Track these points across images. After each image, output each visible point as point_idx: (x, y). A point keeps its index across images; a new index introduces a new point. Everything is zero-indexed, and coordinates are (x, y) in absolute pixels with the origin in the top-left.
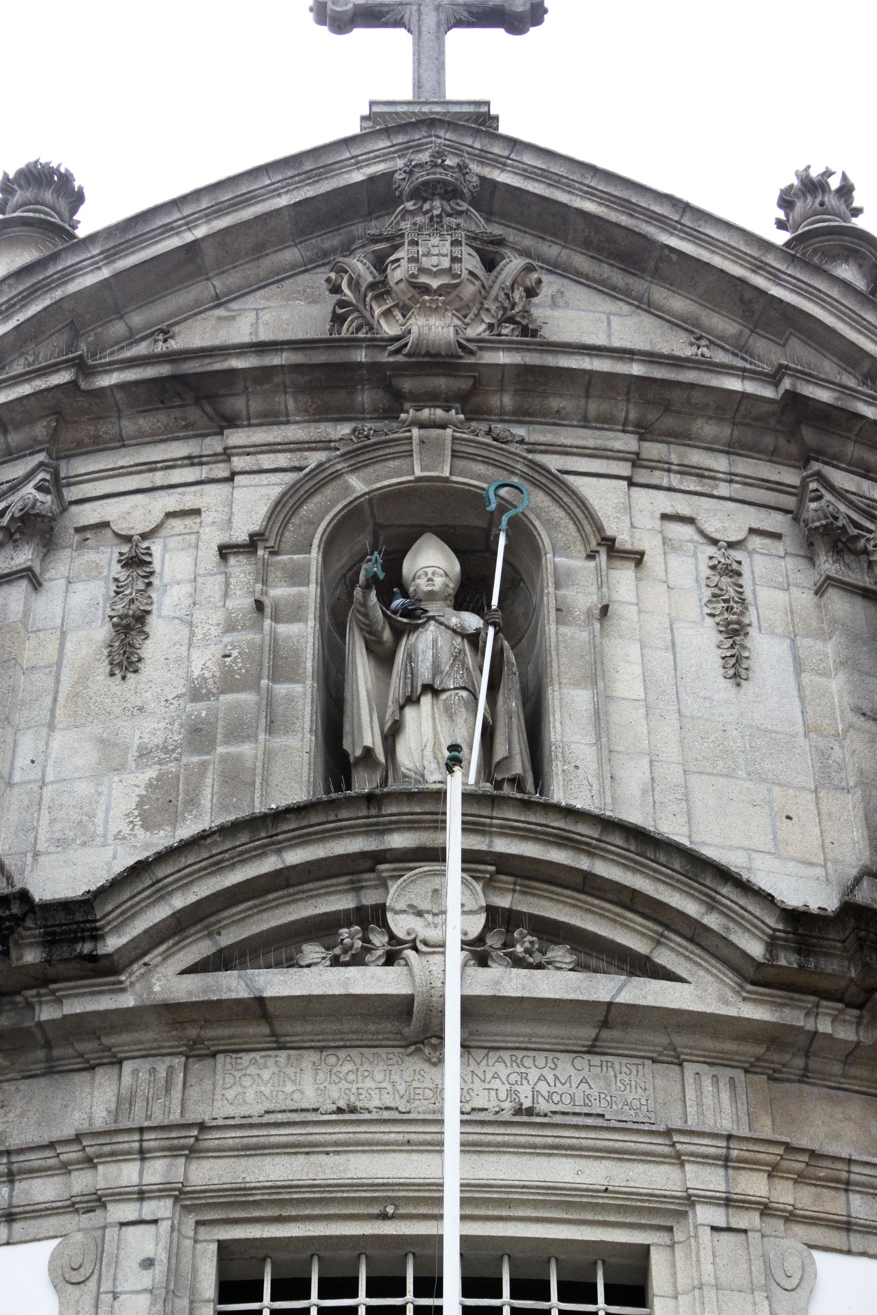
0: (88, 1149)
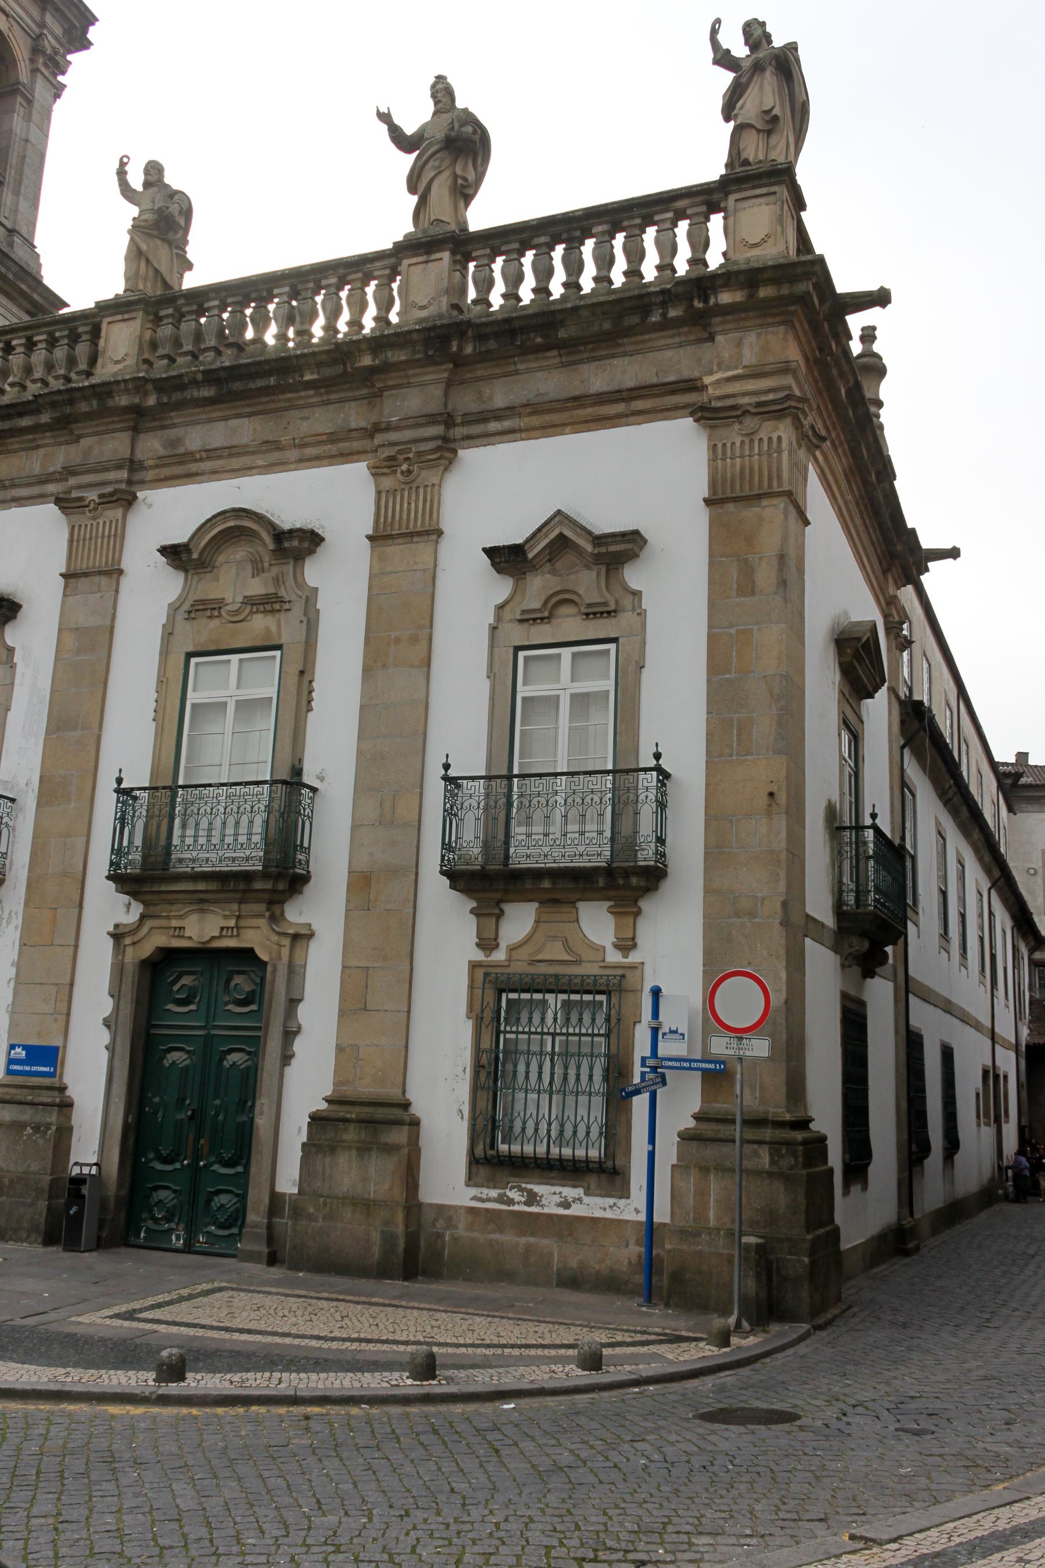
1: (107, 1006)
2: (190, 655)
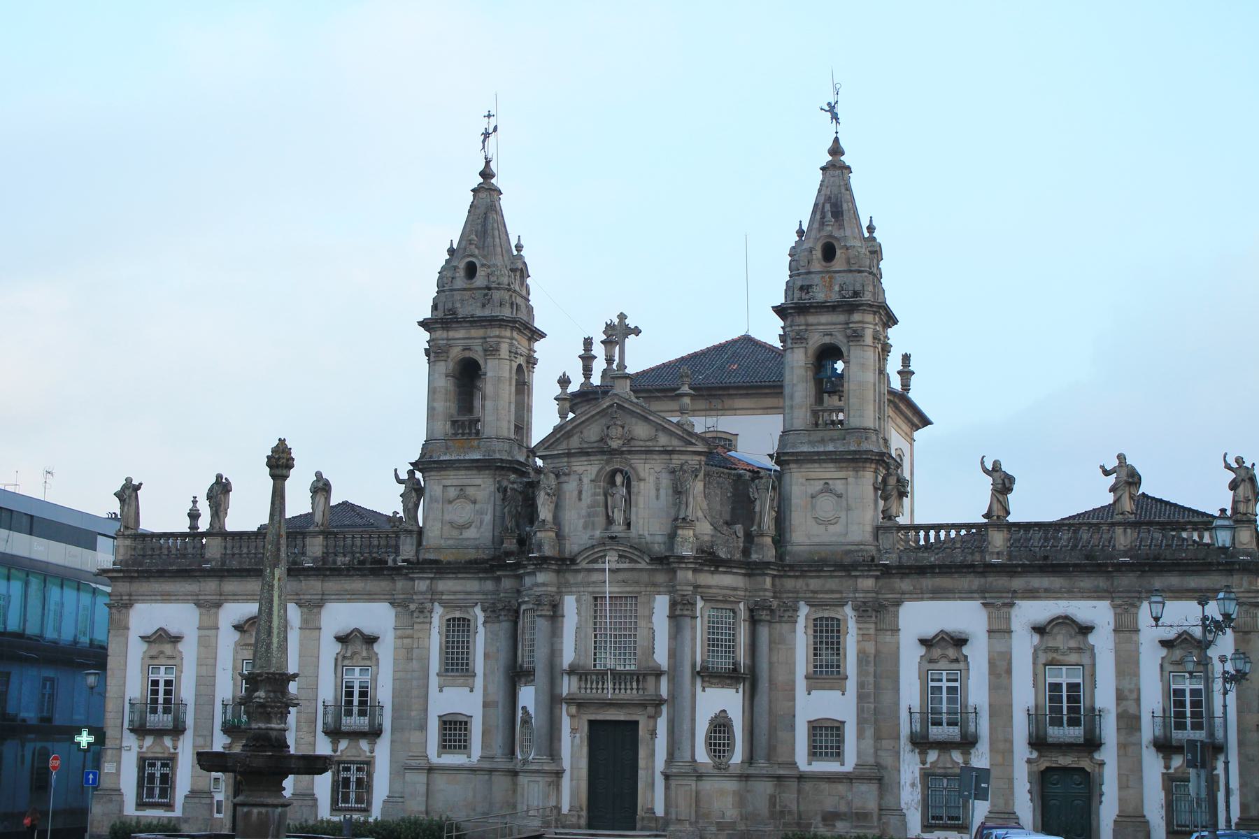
0: (577, 585)
1: (1028, 786)
2: (1045, 665)
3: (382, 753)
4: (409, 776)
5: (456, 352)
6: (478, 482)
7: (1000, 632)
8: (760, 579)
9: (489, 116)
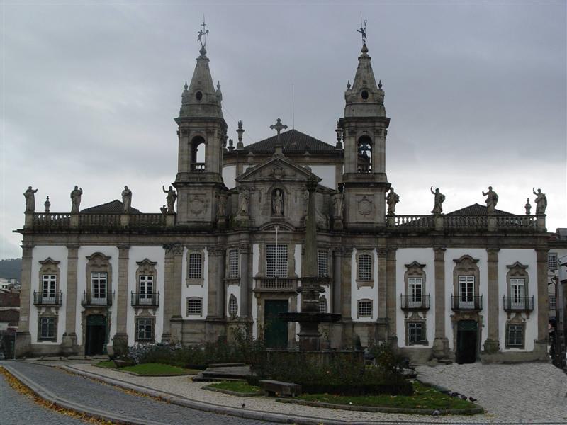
3: (160, 316)
4: (174, 325)
5: (193, 134)
6: (204, 193)
7: (439, 260)
8: (338, 238)
9: (204, 25)
